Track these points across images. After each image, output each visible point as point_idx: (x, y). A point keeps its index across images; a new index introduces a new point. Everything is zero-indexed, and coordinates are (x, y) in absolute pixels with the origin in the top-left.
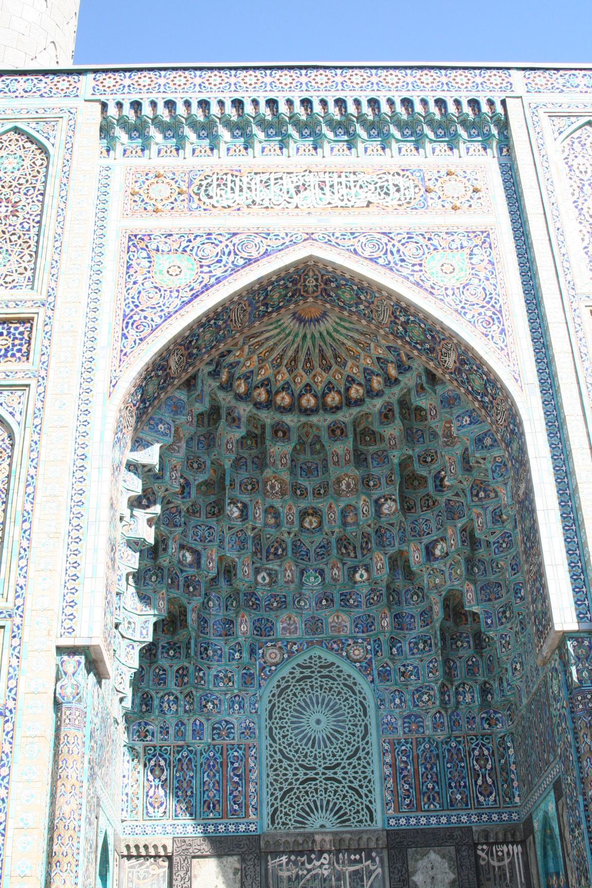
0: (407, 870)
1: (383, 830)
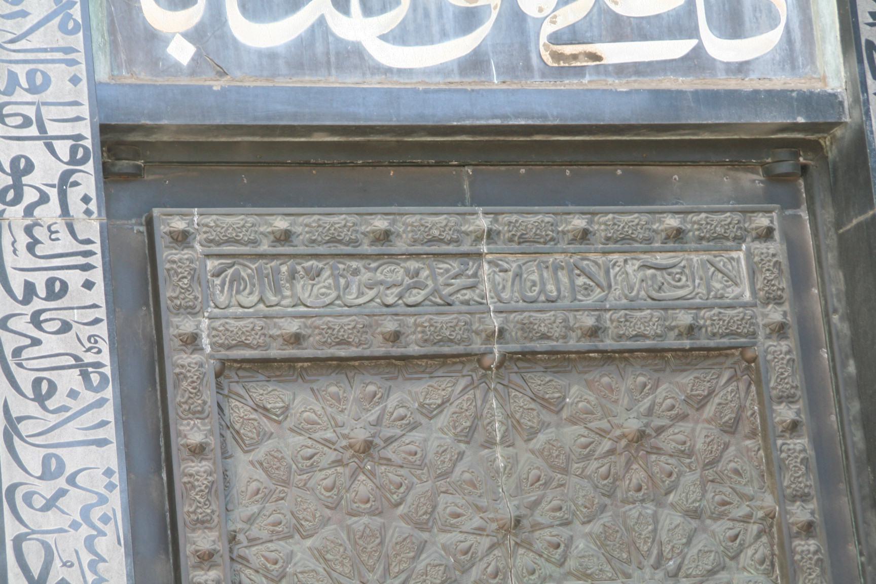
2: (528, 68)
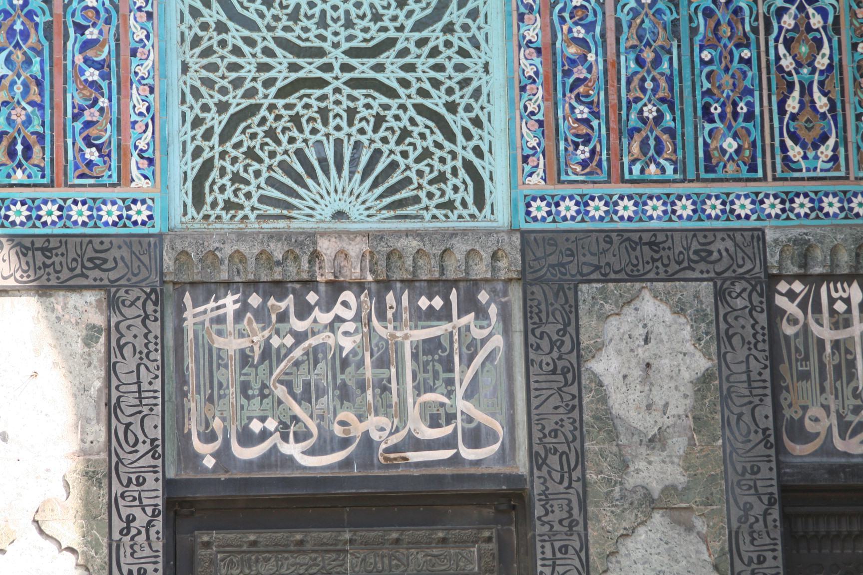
0: (576, 344)
1: (512, 231)
2: (372, 465)
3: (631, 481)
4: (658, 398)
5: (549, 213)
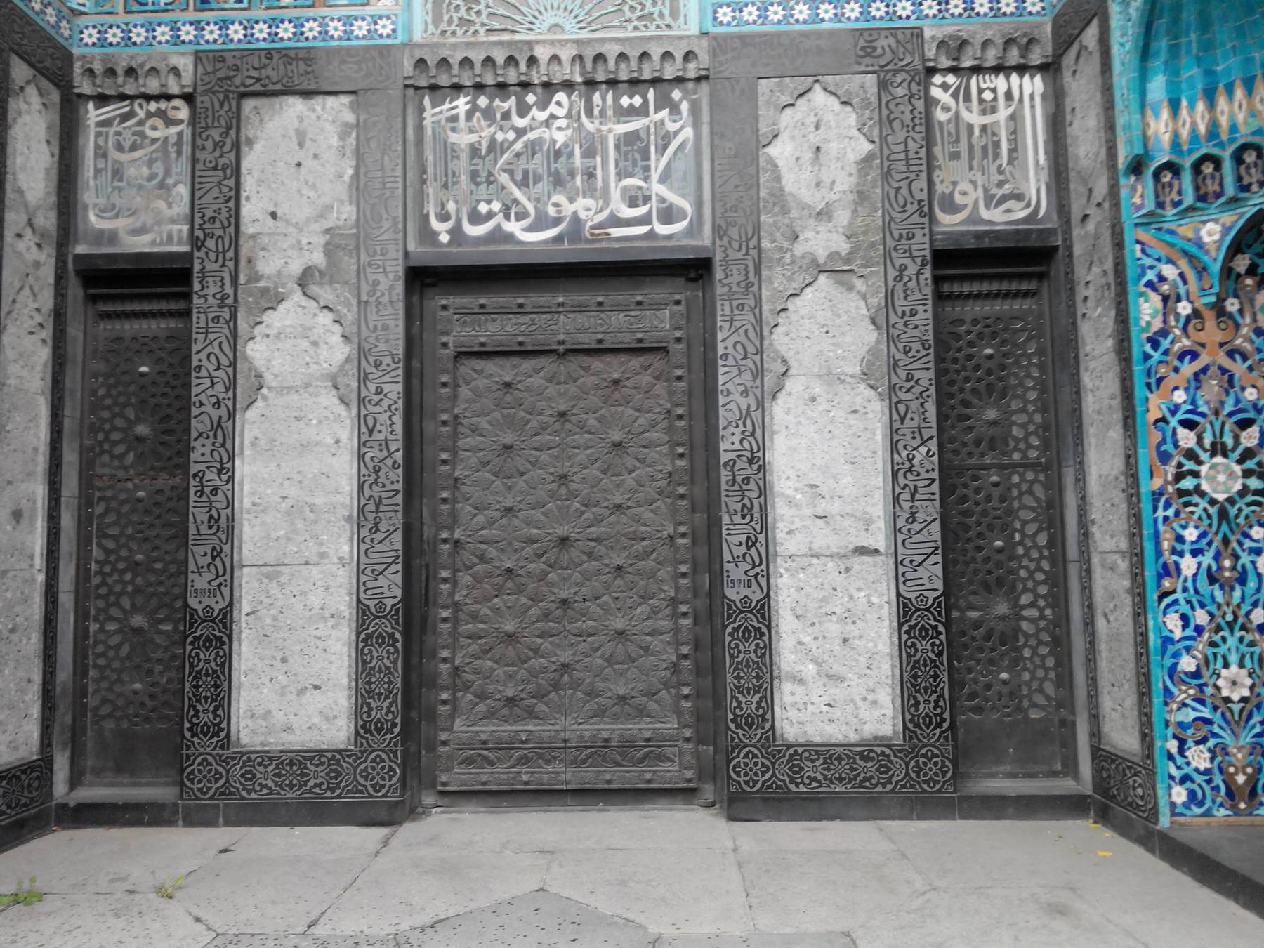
3: (799, 249)
4: (826, 177)
5: (734, 18)
